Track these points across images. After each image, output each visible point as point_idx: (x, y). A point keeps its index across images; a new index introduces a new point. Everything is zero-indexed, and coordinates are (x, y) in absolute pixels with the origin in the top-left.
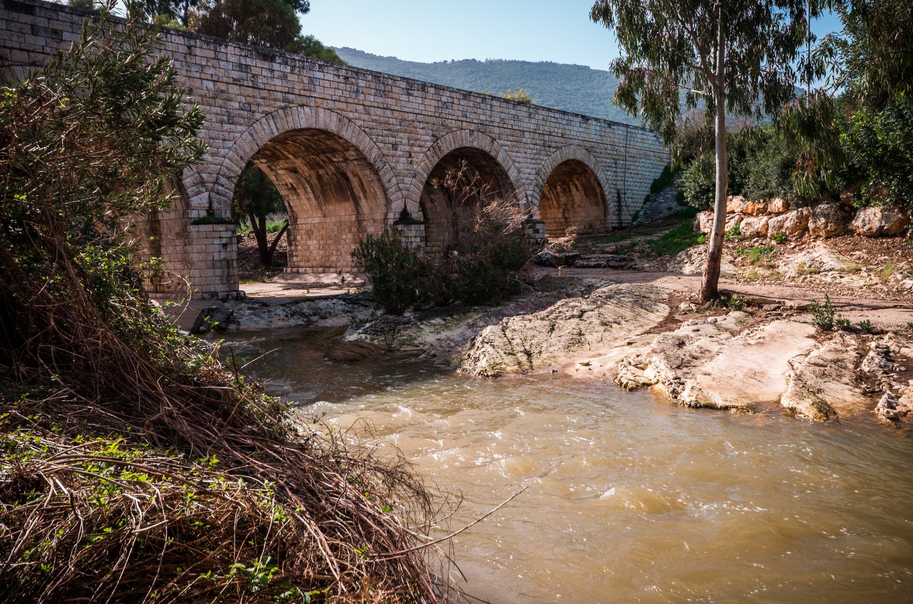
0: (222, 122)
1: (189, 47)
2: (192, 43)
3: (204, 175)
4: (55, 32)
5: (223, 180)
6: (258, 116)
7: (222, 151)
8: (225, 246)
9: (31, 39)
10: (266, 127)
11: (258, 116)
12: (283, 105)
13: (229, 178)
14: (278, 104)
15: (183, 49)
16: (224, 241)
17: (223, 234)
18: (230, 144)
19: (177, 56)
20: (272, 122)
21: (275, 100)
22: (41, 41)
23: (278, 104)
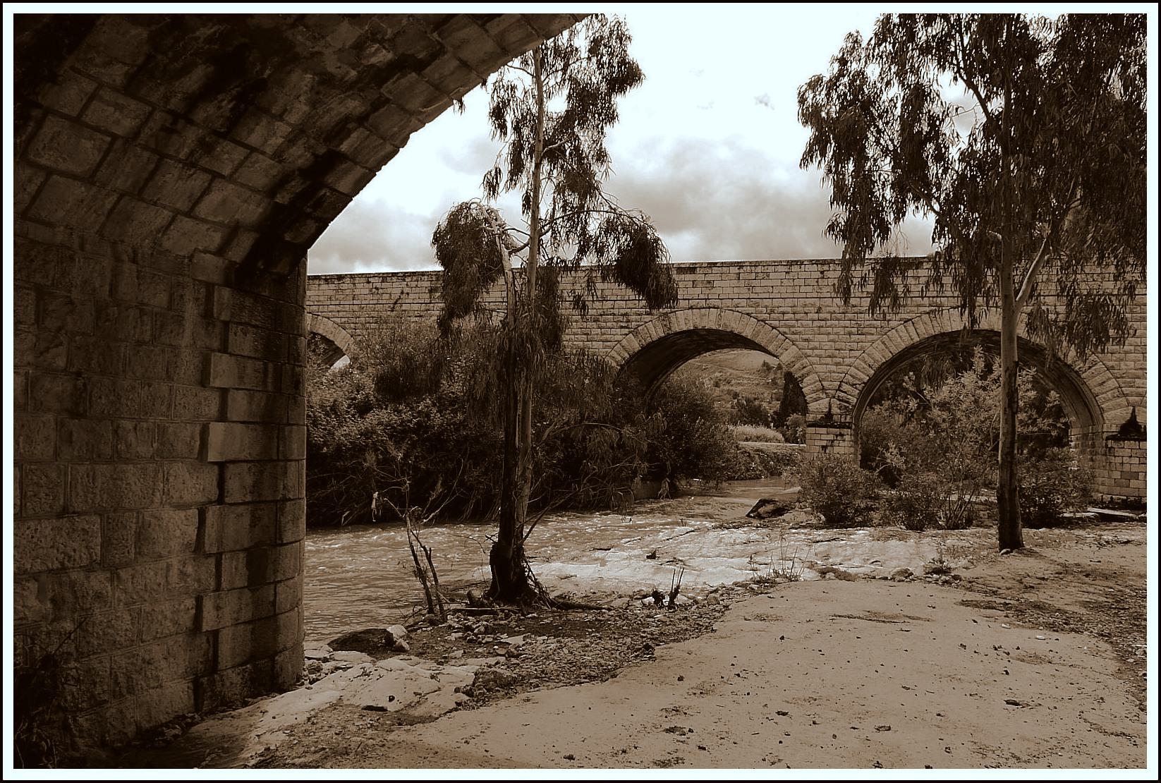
0: (850, 334)
1: (822, 272)
2: (826, 267)
3: (825, 384)
4: (709, 282)
5: (845, 387)
6: (893, 324)
7: (847, 361)
8: (824, 448)
9: (691, 291)
10: (904, 334)
11: (893, 324)
12: (927, 309)
13: (853, 385)
14: (922, 309)
15: (818, 275)
16: (824, 443)
17: (824, 437)
18: (857, 353)
19: (808, 282)
20: (911, 328)
21: (918, 306)
22: (698, 291)
23: (922, 309)
